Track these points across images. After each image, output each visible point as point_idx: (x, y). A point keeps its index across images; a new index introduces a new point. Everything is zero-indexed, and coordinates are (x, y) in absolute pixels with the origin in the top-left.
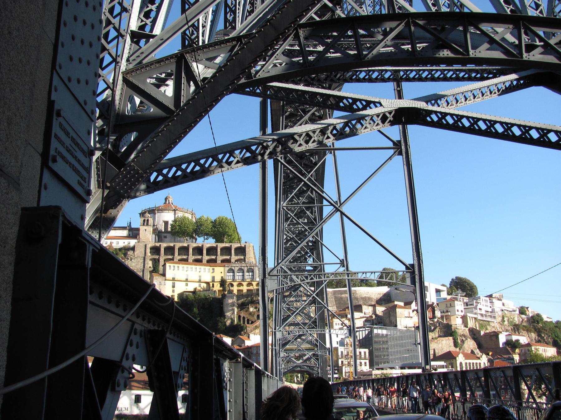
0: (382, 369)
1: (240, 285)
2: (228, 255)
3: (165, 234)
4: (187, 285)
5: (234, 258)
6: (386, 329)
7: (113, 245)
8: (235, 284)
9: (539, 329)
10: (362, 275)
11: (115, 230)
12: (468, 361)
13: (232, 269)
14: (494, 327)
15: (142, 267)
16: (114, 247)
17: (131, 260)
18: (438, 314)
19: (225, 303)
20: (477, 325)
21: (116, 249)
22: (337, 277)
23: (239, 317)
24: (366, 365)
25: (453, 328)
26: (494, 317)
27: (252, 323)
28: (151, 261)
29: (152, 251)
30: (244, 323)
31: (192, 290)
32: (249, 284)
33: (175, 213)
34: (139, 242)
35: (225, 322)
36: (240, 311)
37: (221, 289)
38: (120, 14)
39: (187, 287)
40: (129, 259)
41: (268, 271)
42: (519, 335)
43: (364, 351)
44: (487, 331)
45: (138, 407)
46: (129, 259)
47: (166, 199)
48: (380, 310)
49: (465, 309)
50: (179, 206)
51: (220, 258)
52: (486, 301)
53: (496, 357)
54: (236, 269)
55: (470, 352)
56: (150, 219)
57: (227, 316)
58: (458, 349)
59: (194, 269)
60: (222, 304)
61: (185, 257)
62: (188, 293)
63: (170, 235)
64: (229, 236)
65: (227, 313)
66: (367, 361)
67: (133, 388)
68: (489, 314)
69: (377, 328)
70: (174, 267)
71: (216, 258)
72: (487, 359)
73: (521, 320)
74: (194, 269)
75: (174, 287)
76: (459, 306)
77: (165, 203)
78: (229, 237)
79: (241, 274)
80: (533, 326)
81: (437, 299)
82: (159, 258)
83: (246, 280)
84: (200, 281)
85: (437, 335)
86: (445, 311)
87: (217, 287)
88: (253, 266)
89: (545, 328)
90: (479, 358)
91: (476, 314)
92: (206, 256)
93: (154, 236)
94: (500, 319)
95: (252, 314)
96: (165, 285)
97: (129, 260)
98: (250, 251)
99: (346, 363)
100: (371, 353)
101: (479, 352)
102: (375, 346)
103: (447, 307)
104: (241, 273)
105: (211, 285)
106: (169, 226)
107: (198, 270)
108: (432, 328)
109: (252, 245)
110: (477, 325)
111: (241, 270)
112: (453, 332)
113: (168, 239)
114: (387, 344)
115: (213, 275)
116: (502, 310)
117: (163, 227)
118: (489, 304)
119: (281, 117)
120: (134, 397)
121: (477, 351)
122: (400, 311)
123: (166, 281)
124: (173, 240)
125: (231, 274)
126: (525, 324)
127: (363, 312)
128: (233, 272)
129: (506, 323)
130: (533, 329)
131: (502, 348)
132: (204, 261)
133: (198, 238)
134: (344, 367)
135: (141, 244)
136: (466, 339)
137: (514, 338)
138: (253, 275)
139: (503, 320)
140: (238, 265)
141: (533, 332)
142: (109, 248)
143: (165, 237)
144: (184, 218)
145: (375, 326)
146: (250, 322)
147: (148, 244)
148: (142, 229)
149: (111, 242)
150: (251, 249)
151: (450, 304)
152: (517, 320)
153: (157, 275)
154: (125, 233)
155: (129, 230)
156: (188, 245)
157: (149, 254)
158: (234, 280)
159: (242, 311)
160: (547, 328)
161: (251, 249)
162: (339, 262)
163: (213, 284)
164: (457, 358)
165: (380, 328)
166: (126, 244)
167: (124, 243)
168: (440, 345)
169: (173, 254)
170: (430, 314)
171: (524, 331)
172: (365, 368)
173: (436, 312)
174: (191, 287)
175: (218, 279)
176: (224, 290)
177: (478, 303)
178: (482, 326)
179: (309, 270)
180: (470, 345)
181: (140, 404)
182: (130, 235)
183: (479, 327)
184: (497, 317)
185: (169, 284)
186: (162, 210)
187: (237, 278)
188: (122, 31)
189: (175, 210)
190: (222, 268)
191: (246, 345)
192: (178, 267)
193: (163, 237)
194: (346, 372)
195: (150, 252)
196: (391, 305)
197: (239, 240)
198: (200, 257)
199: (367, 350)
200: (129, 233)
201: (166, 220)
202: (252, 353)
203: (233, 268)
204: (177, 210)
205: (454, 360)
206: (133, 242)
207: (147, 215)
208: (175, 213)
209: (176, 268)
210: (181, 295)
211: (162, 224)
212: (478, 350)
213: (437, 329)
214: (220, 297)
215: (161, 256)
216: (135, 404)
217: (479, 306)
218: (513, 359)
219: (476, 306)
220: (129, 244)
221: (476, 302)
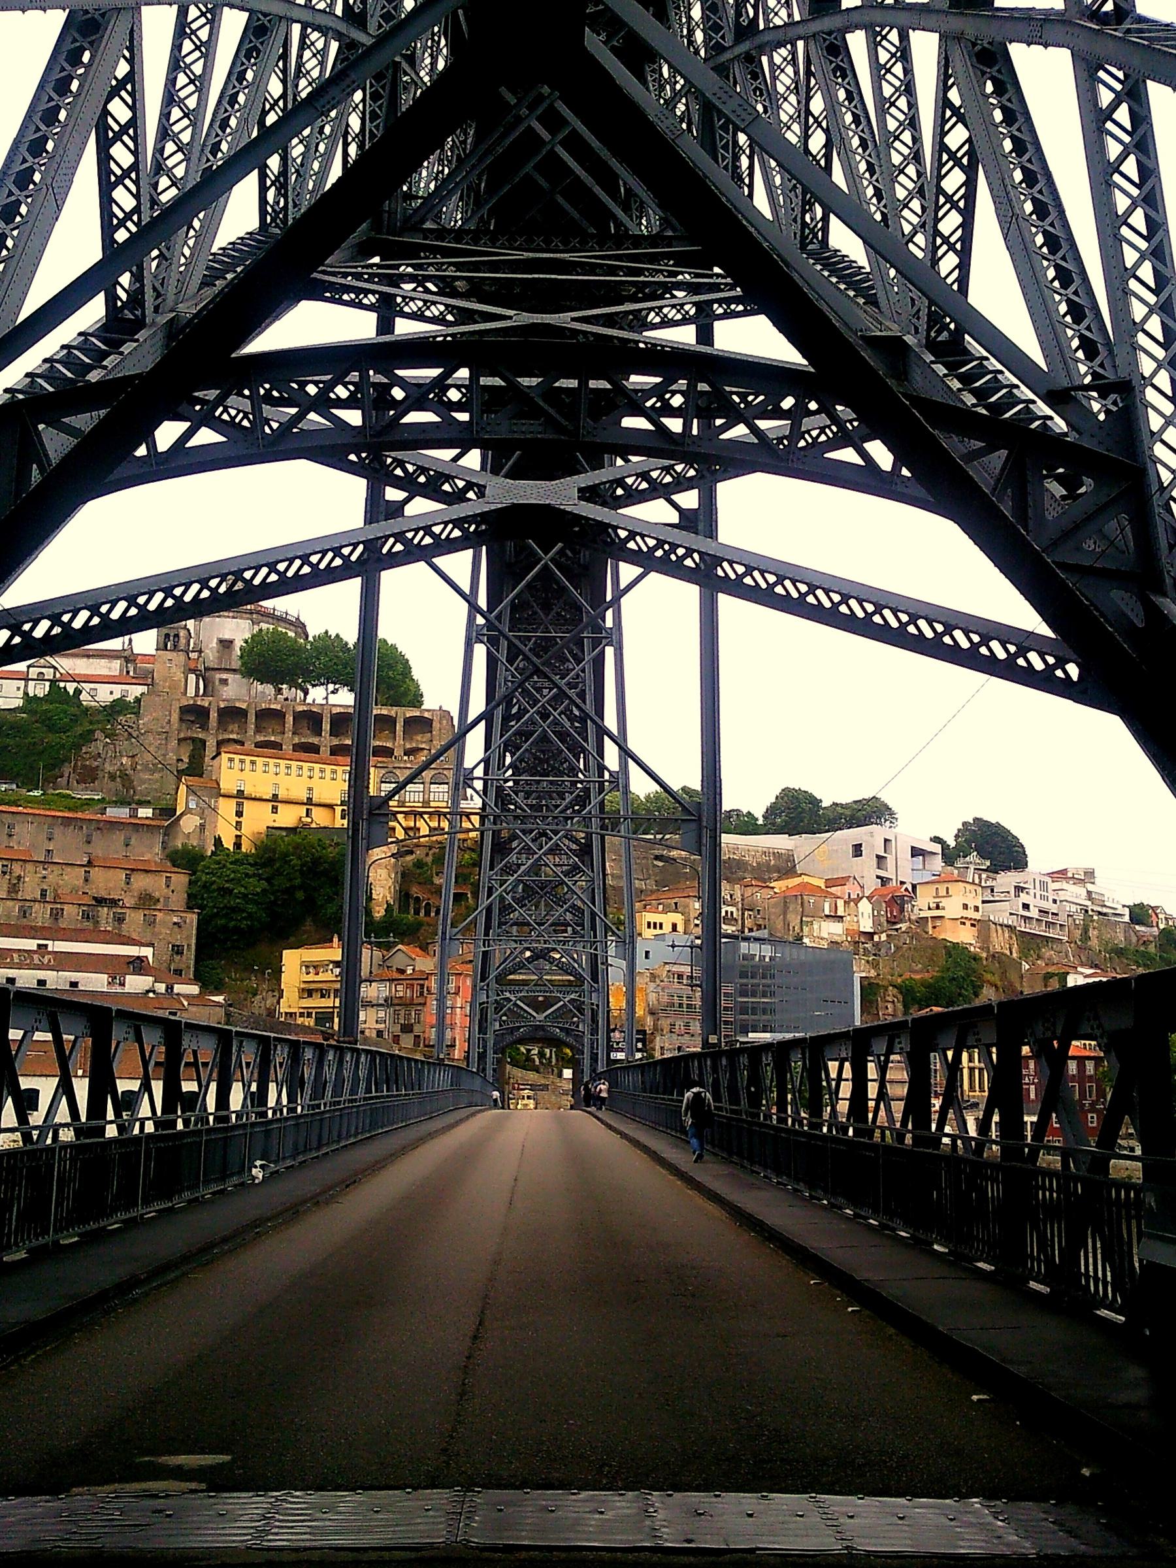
4: (275, 810)
62: (278, 833)
75: (239, 814)
167: (111, 693)
174: (288, 817)
185: (227, 808)
192: (253, 763)
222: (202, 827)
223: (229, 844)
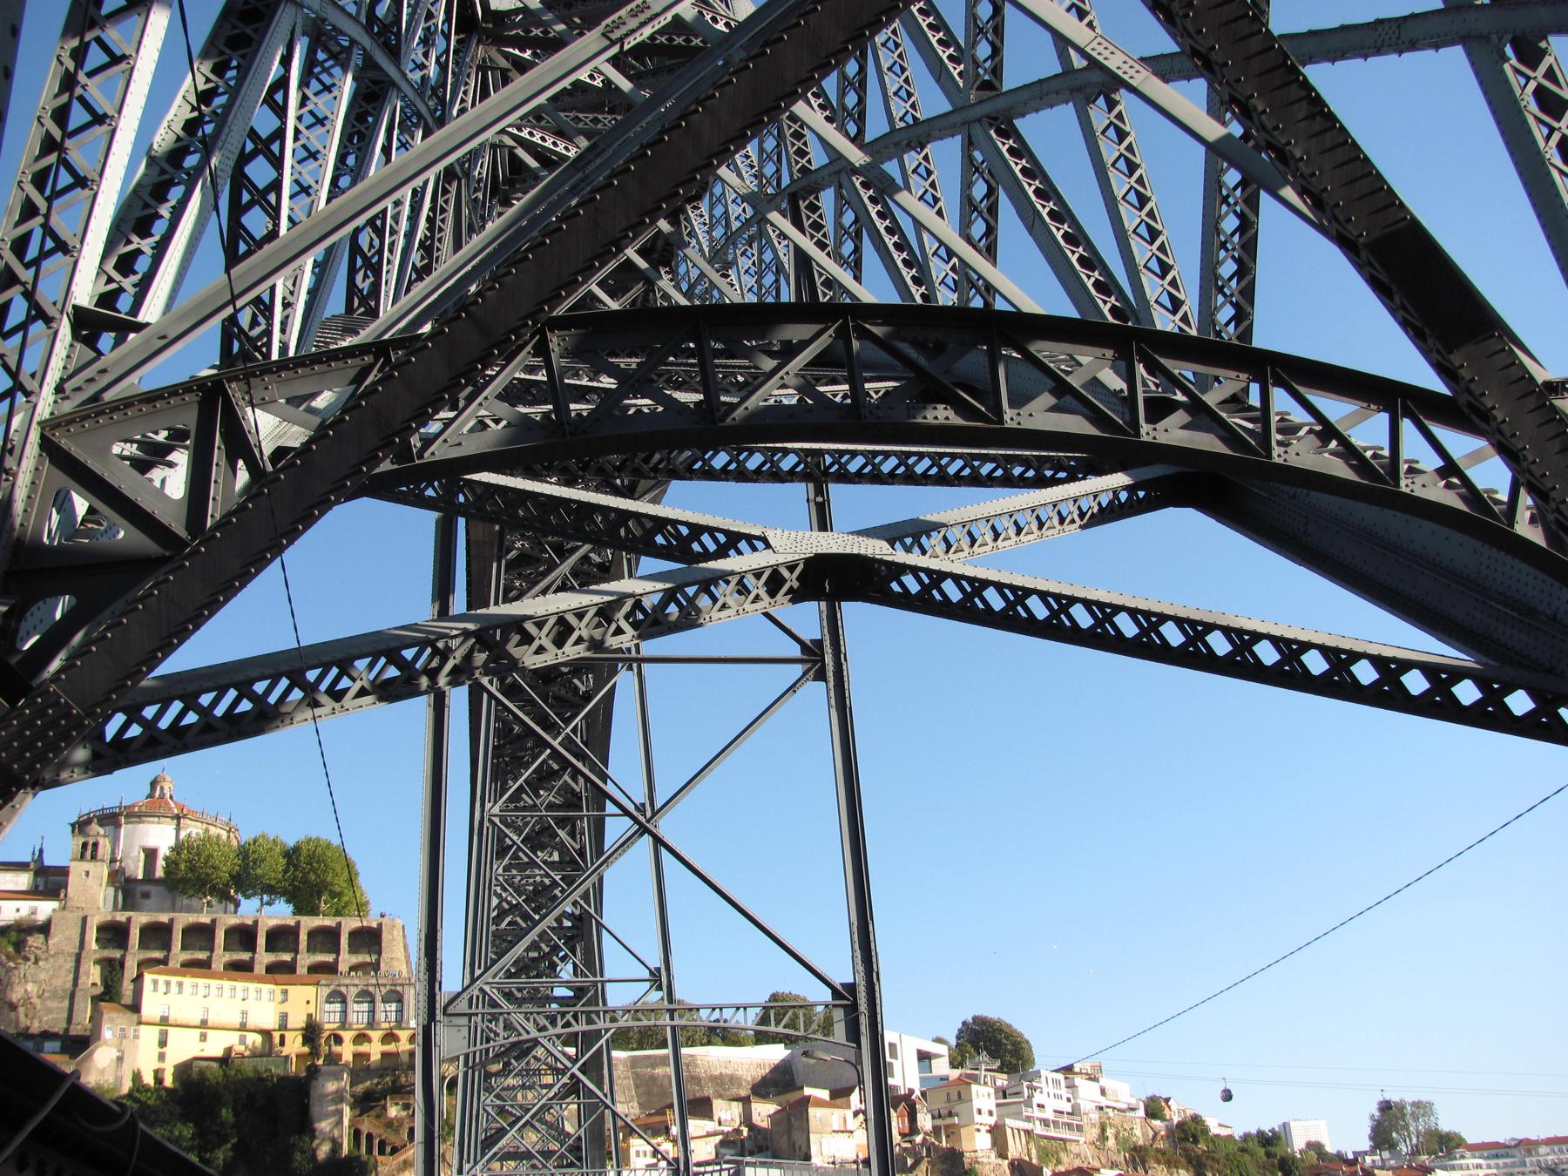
1: (361, 1038)
2: (330, 952)
3: (147, 888)
4: (203, 1038)
5: (346, 959)
8: (348, 1036)
9: (1198, 1157)
10: (710, 1015)
14: (1078, 1155)
15: (69, 985)
17: (36, 962)
18: (925, 1121)
19: (314, 1094)
20: (1034, 1151)
25: (966, 1161)
26: (1080, 1128)
27: (395, 1150)
28: (98, 968)
29: (102, 936)
30: (370, 1150)
31: (219, 1053)
32: (390, 1037)
33: (178, 824)
34: (64, 908)
35: (314, 1151)
36: (360, 1115)
37: (306, 1049)
38: (23, 327)
39: (203, 1045)
40: (29, 959)
41: (441, 1000)
44: (1061, 1168)
46: (29, 959)
47: (154, 784)
48: (763, 1111)
49: (998, 1105)
50: (191, 805)
51: (305, 960)
52: (1056, 1083)
54: (352, 992)
56: (101, 841)
57: (322, 1132)
59: (226, 991)
60: (307, 1094)
61: (202, 955)
62: (205, 1063)
64: (334, 895)
65: (320, 1121)
68: (1066, 1119)
70: (168, 983)
71: (294, 960)
73: (1151, 1133)
74: (226, 991)
75: (163, 1043)
76: (983, 1098)
77: (151, 796)
78: (333, 898)
79: (365, 1007)
80: (1185, 1149)
82: (123, 957)
83: (379, 1023)
84: (243, 1027)
87: (294, 1045)
89: (1216, 1156)
91: (1028, 1119)
92: (264, 954)
93: (111, 890)
94: (1095, 1132)
95: (395, 1124)
96: (137, 1037)
97: (29, 963)
98: (393, 940)
103: (949, 1100)
104: (366, 1005)
105: (277, 1040)
106: (161, 863)
107: (240, 994)
108: (910, 1162)
109: (399, 922)
110: (1034, 1151)
111: (366, 996)
112: (966, 1173)
116: (1101, 1108)
117: (141, 864)
118: (1064, 1092)
119: (495, 565)
122: (818, 1115)
123: (142, 1027)
124: (168, 904)
125: (338, 1007)
126: (1160, 1145)
127: (716, 1118)
128: (344, 1001)
129: (1111, 1143)
130: (1182, 1160)
132: (259, 969)
133: (244, 901)
135: (70, 915)
138: (402, 1011)
139: (1103, 1137)
140: (357, 982)
141: (1183, 1168)
143: (146, 895)
144: (207, 839)
145: (748, 1159)
146: (388, 1149)
147: (93, 916)
148: (77, 869)
150: (397, 933)
151: (959, 1094)
152: (1140, 1133)
153: (112, 1009)
154: (23, 881)
155: (37, 873)
157: (94, 946)
158: (344, 1024)
159: (365, 1117)
160: (1220, 1155)
161: (397, 933)
162: (646, 974)
163: (282, 1038)
167: (18, 910)
169: (167, 946)
170: (903, 1123)
171: (1159, 1163)
173: (920, 1116)
174: (216, 1046)
175: (298, 1020)
178: (1045, 1154)
179: (563, 998)
182: (37, 887)
183: (1039, 1157)
184: (1086, 1128)
185: (149, 1035)
186: (140, 816)
187: (352, 1018)
188: (24, 377)
189: (178, 818)
190: (311, 990)
192: (180, 984)
195: (97, 940)
196: (793, 1097)
197: (361, 909)
198: (246, 956)
201: (151, 843)
203: (343, 989)
206: (45, 909)
207: (95, 828)
208: (178, 824)
210: (183, 1070)
211: (139, 857)
213: (923, 1166)
215: (130, 950)
217: (1038, 1098)
219: (1030, 1097)
220: (34, 912)
222: (120, 1059)
223: (149, 1079)
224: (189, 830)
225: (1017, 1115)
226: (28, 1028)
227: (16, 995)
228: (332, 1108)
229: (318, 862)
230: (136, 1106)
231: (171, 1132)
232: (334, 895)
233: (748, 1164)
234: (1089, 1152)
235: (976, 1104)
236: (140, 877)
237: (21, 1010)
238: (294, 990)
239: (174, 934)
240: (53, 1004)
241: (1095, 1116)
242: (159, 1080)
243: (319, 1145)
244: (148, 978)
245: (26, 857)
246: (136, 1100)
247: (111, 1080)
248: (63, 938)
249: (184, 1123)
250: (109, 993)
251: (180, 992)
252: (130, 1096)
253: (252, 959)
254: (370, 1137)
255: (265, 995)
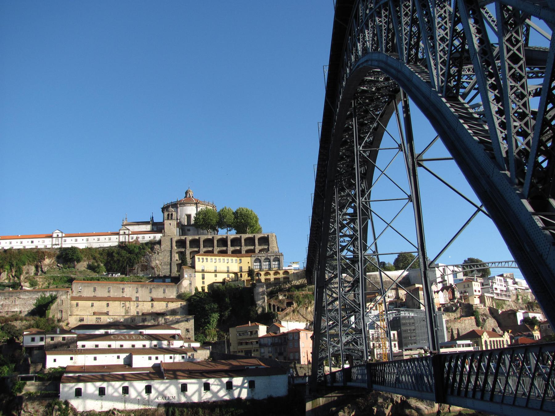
0: (411, 350)
1: (267, 274)
2: (252, 245)
3: (189, 228)
4: (216, 276)
5: (258, 248)
6: (412, 311)
7: (139, 240)
8: (262, 273)
11: (139, 225)
12: (492, 339)
13: (259, 259)
14: (509, 305)
15: (169, 261)
16: (140, 242)
17: (158, 254)
18: (457, 295)
19: (255, 292)
20: (494, 304)
21: (142, 244)
22: (478, 267)
23: (270, 305)
24: (395, 347)
25: (474, 308)
26: (509, 296)
27: (282, 310)
28: (177, 254)
30: (274, 310)
31: (221, 281)
32: (276, 273)
33: (197, 206)
35: (257, 311)
36: (270, 299)
37: (249, 278)
39: (216, 278)
40: (155, 253)
41: (428, 263)
42: (533, 312)
43: (394, 333)
44: (504, 310)
45: (185, 395)
46: (155, 253)
47: (186, 193)
48: (402, 293)
49: (481, 289)
50: (200, 200)
51: (244, 249)
52: (501, 280)
53: (516, 334)
55: (491, 330)
56: (174, 213)
57: (259, 305)
58: (480, 328)
59: (222, 261)
60: (253, 293)
61: (210, 249)
62: (218, 284)
63: (194, 227)
64: (251, 227)
66: (397, 343)
67: (179, 377)
68: (504, 293)
69: (403, 311)
70: (203, 259)
71: (241, 249)
72: (509, 336)
74: (222, 261)
75: (203, 278)
76: (476, 286)
77: (186, 197)
79: (267, 263)
81: (454, 280)
82: (185, 251)
83: (272, 269)
84: (228, 272)
85: (459, 315)
86: (463, 291)
87: (245, 277)
88: (279, 255)
90: (501, 336)
91: (492, 293)
93: (178, 229)
94: (514, 297)
96: (195, 276)
98: (273, 240)
99: (377, 345)
100: (399, 335)
101: (500, 330)
102: (403, 328)
103: (465, 287)
105: (239, 276)
106: (193, 219)
107: (226, 261)
108: (454, 308)
109: (274, 234)
110: (494, 304)
113: (191, 232)
114: (414, 325)
115: (241, 265)
116: (516, 289)
117: (186, 220)
118: (503, 284)
119: (354, 119)
120: (180, 386)
121: (498, 329)
124: (196, 233)
125: (258, 264)
128: (260, 262)
129: (520, 301)
131: (520, 325)
132: (229, 252)
133: (219, 229)
134: (375, 350)
136: (488, 318)
137: (531, 315)
138: (280, 264)
139: (517, 299)
140: (264, 255)
142: (136, 243)
143: (189, 230)
145: (401, 309)
146: (280, 310)
147: (174, 238)
148: (167, 223)
149: (137, 237)
150: (274, 238)
151: (468, 285)
153: (186, 268)
154: (148, 228)
156: (213, 237)
157: (175, 248)
158: (261, 269)
159: (271, 299)
161: (274, 238)
163: (241, 275)
164: (482, 337)
165: (406, 310)
166: (152, 238)
167: (150, 237)
168: (463, 325)
169: (199, 246)
171: (538, 308)
172: (396, 350)
174: (220, 278)
175: (245, 269)
176: (252, 279)
177: (494, 283)
178: (498, 305)
180: (491, 323)
181: (187, 393)
182: (153, 229)
183: (496, 306)
185: (199, 276)
187: (264, 267)
189: (196, 204)
190: (249, 258)
191: (281, 331)
192: (207, 259)
193: (186, 230)
194: (377, 354)
196: (412, 288)
197: (259, 231)
198: (225, 248)
199: (395, 332)
200: (152, 227)
201: (188, 213)
202: (288, 340)
203: (260, 258)
204: (199, 203)
205: (479, 339)
206: (158, 236)
207: (171, 209)
208: (197, 206)
209: (205, 260)
210: (211, 286)
212: (499, 328)
213: (459, 310)
214: (249, 286)
216: (182, 393)
217: (495, 286)
218: (532, 336)
219: (492, 286)
220: (155, 238)
221: (491, 282)
222: (190, 284)
223: (200, 290)
224: (201, 208)
225: (488, 292)
226: (159, 275)
227: (153, 264)
228: (261, 297)
229: (244, 216)
230: (198, 298)
231: (211, 306)
232: (251, 227)
233: (402, 311)
234: (512, 304)
235: (474, 288)
236: (186, 224)
237: (156, 269)
238: (243, 259)
239: (201, 243)
240: (165, 267)
241: (514, 292)
242: (203, 290)
243: (259, 309)
244: (196, 257)
245: (149, 220)
246: (198, 297)
247: (189, 290)
248: (166, 245)
249: (214, 303)
250: (183, 263)
251: (207, 261)
252: (195, 295)
253: (227, 249)
254: (274, 306)
255: (234, 261)
